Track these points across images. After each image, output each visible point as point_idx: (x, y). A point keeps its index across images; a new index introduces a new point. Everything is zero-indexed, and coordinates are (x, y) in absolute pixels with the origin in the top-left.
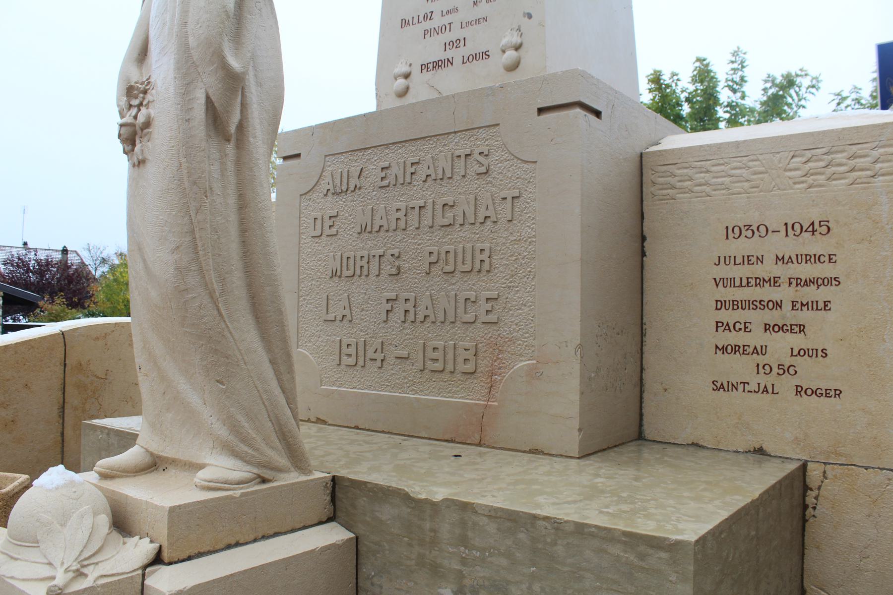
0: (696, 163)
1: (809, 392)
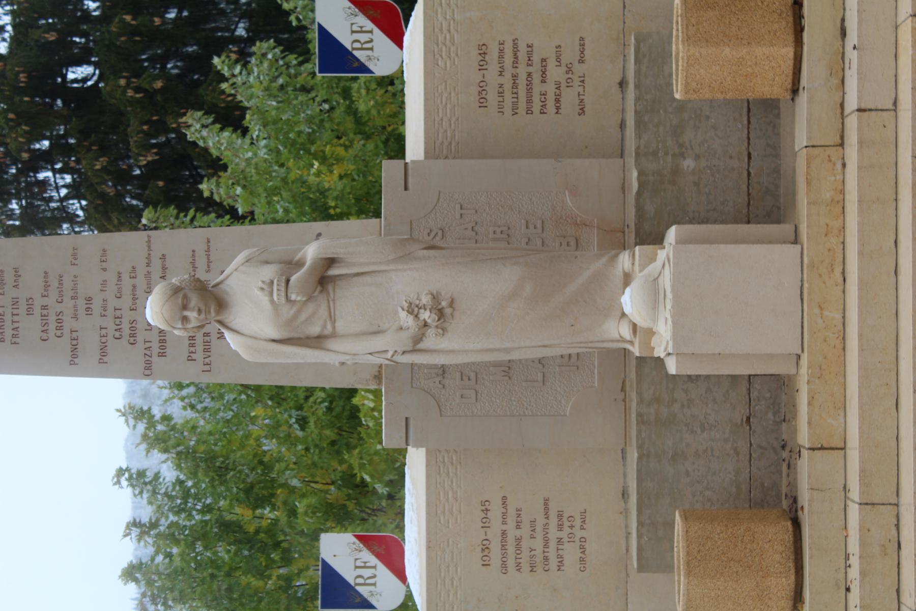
1: (582, 55)
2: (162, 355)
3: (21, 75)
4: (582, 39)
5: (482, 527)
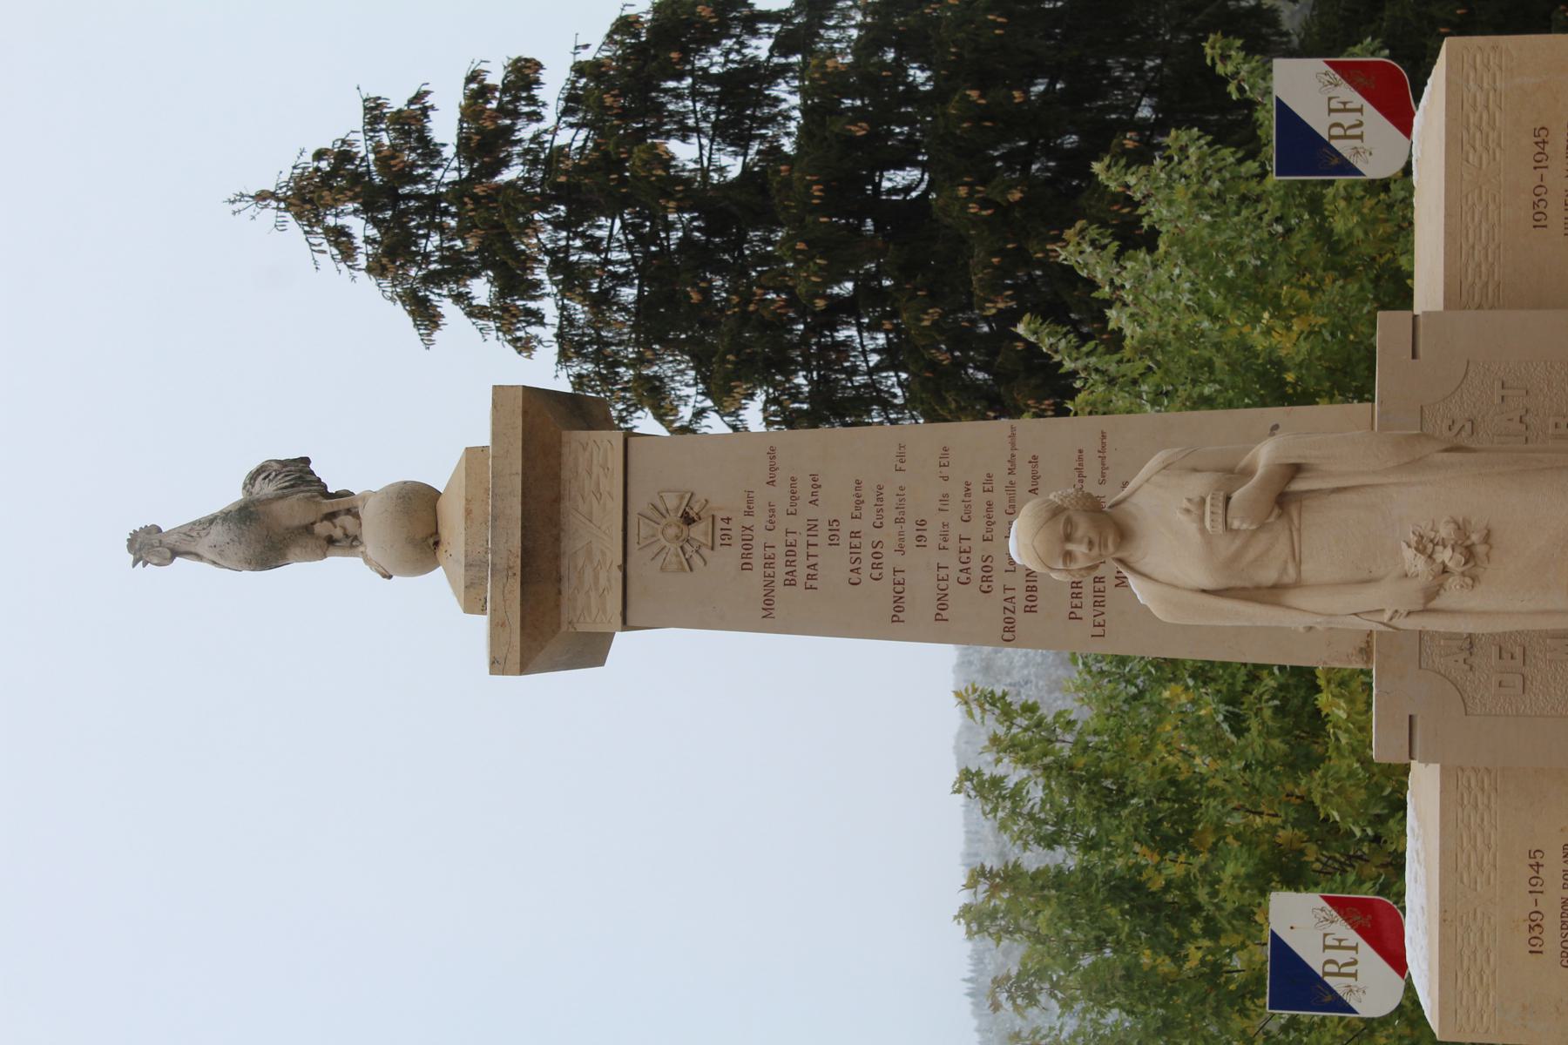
2: (1030, 610)
3: (815, 187)
5: (1530, 892)
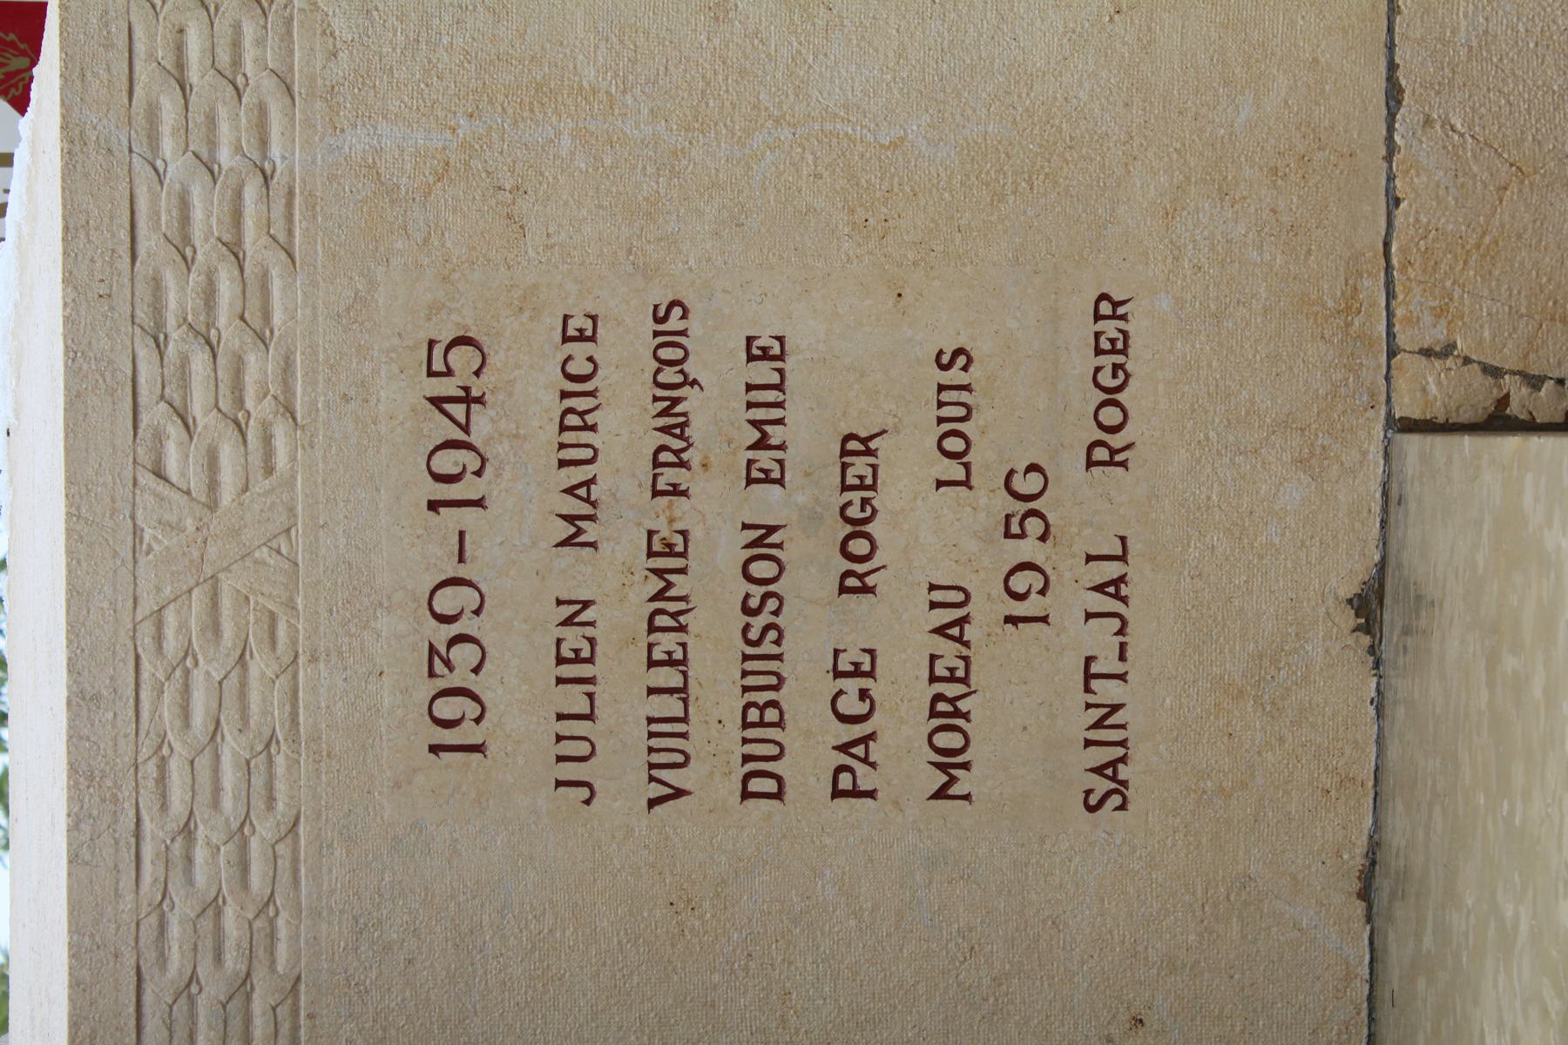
0: (147, 878)
1: (1111, 416)
4: (1108, 307)
